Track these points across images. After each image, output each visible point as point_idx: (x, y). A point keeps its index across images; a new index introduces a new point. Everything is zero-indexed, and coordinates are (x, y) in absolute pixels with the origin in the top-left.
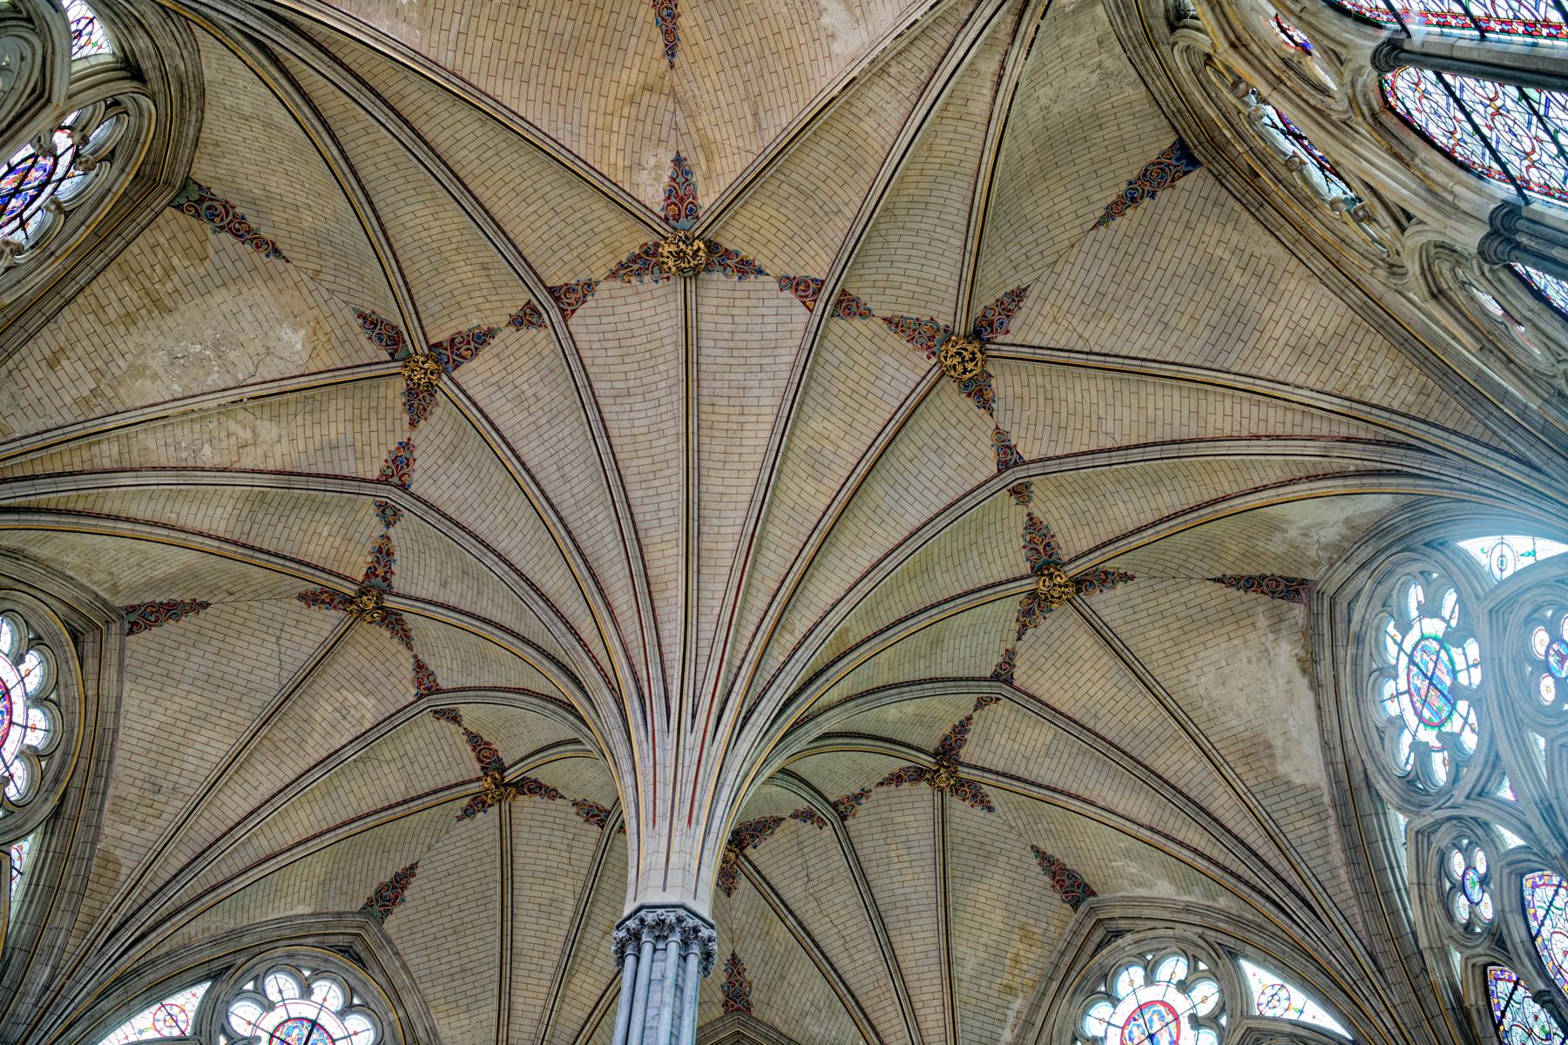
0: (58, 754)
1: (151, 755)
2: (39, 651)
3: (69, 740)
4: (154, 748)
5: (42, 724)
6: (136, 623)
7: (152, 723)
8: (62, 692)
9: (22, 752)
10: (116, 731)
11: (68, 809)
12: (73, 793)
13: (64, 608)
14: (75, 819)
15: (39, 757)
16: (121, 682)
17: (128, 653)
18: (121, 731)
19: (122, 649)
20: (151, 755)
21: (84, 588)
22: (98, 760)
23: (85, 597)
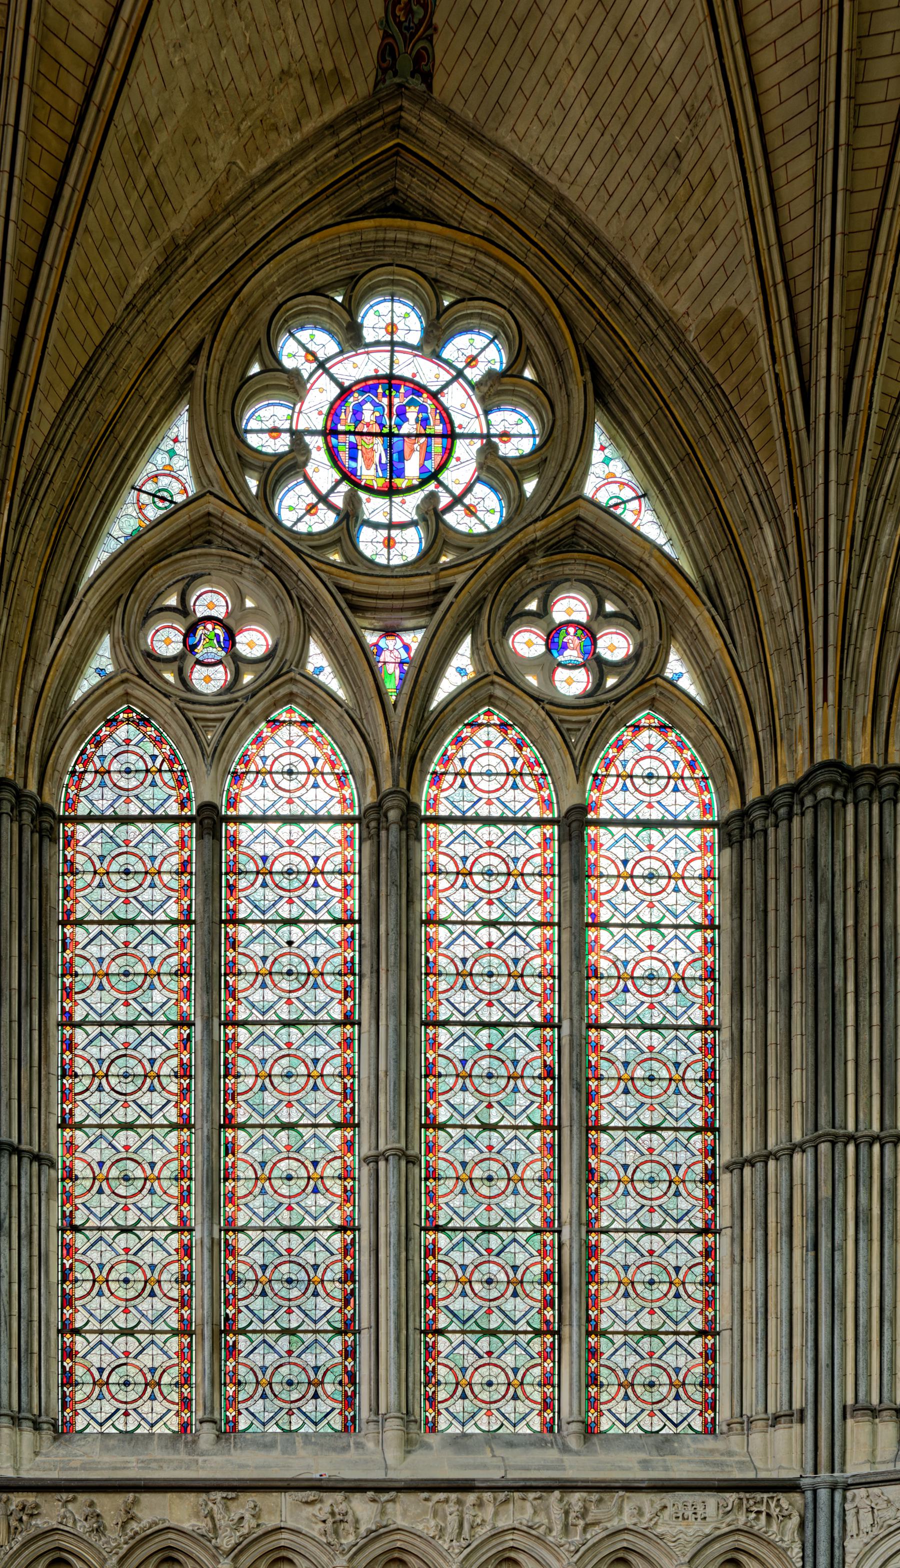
0: (533, 337)
1: (622, 142)
2: (371, 291)
3: (526, 306)
4: (614, 129)
5: (480, 340)
6: (418, 59)
7: (576, 111)
8: (453, 278)
9: (483, 399)
10: (560, 203)
11: (610, 362)
12: (598, 344)
13: (326, 209)
14: (630, 361)
15: (512, 372)
16: (492, 147)
17: (457, 106)
18: (564, 190)
19: (449, 117)
20: (622, 142)
21: (300, 152)
22: (581, 264)
23: (324, 153)
